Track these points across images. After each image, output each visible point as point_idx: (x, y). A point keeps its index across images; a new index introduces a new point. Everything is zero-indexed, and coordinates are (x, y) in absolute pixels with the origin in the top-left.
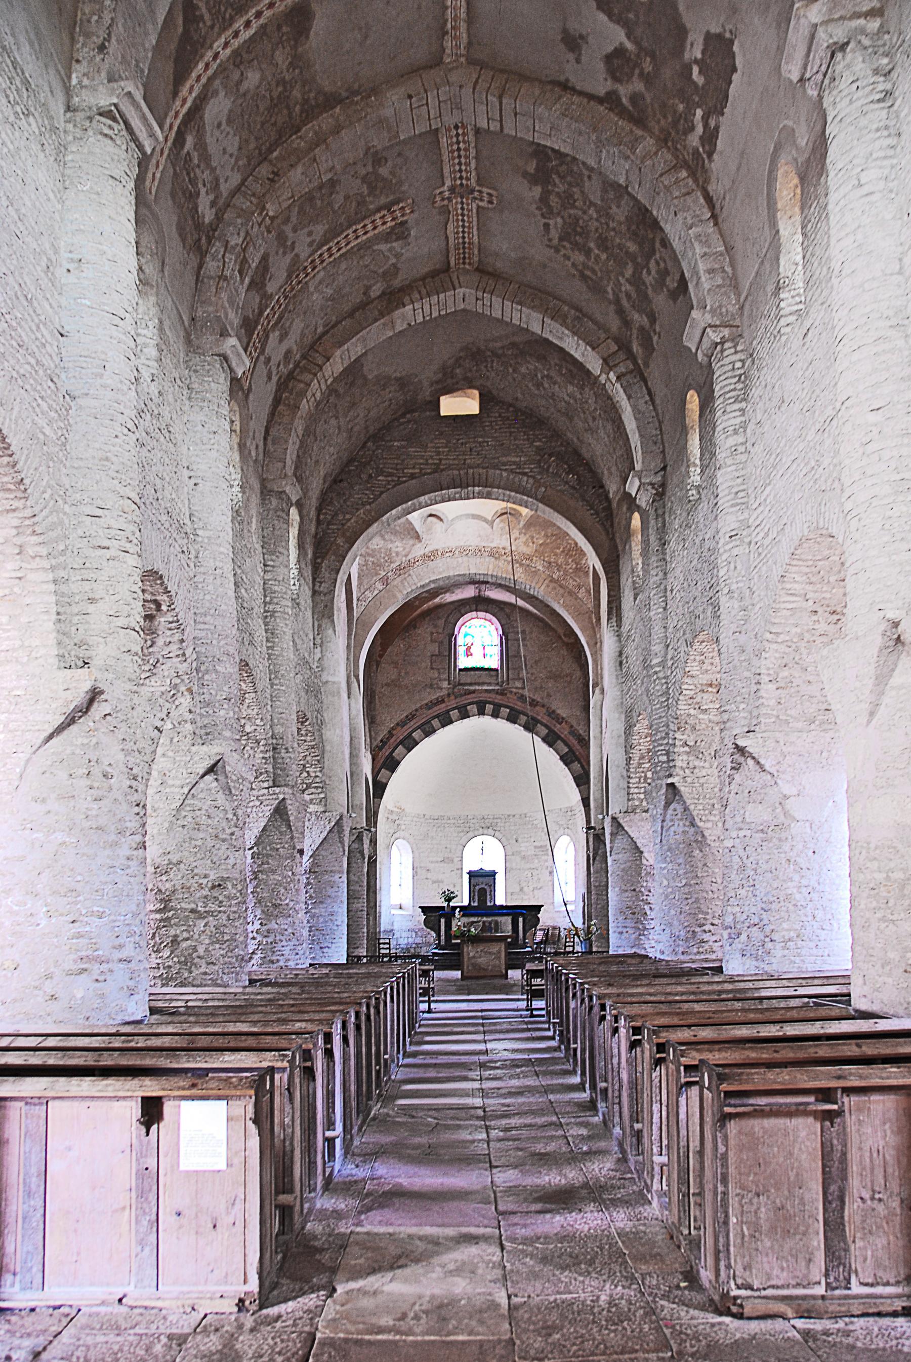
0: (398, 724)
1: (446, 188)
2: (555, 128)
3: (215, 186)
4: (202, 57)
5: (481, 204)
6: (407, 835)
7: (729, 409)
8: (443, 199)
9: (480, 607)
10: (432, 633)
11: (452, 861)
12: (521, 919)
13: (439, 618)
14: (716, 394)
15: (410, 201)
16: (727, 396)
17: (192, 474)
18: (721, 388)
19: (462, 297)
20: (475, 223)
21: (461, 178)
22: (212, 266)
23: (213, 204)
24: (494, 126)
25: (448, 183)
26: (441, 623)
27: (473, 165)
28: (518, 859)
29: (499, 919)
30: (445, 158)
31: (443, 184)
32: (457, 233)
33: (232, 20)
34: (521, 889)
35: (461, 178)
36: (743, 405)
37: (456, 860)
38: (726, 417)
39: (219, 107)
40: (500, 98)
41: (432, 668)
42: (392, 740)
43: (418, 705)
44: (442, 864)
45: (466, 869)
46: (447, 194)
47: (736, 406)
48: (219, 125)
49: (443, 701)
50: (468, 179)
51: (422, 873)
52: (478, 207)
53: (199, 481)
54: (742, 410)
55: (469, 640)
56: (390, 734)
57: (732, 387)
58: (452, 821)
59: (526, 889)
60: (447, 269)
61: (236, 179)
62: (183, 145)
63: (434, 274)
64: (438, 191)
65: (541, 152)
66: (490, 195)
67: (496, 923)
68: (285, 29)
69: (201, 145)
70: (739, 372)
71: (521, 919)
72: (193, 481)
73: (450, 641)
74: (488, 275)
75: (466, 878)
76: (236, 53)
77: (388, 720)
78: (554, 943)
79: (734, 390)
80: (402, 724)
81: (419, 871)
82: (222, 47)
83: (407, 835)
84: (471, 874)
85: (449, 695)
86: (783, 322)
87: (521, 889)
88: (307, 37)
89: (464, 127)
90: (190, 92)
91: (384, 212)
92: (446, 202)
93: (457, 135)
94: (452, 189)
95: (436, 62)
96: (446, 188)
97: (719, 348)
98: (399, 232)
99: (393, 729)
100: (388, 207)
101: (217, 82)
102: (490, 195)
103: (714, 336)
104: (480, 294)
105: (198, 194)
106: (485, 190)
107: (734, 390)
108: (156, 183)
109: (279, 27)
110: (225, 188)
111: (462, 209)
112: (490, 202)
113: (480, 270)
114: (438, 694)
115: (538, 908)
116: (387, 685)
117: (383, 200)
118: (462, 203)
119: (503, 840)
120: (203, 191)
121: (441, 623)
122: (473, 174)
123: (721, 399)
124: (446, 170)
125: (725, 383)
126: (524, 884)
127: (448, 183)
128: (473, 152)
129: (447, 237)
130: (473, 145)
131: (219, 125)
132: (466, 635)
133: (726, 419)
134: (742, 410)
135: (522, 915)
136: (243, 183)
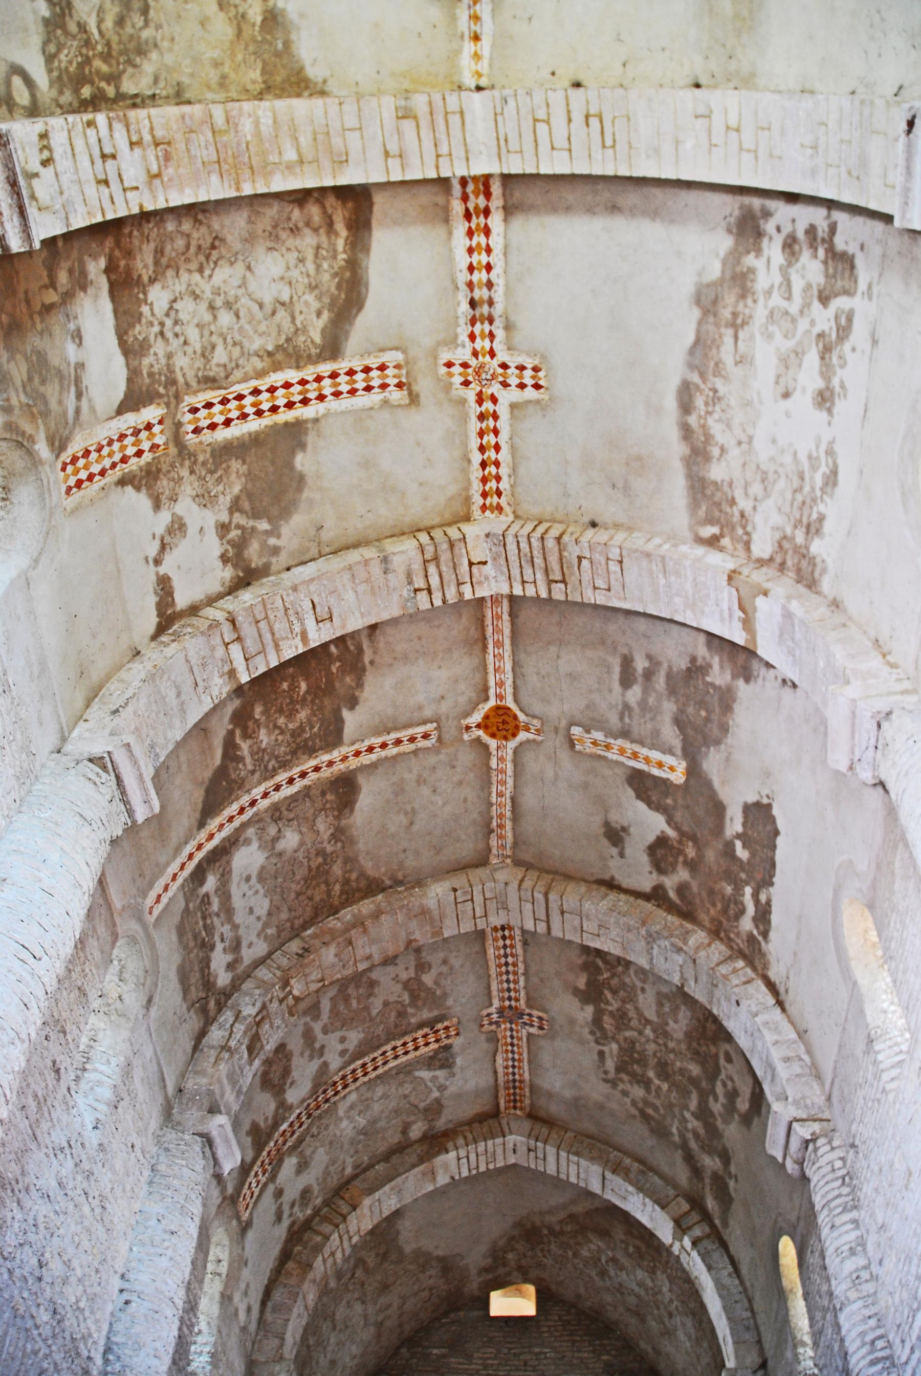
1: (493, 1010)
2: (606, 926)
3: (236, 946)
4: (237, 799)
5: (532, 1030)
7: (838, 1221)
8: (491, 1023)
14: (818, 1207)
15: (455, 1020)
16: (833, 1204)
17: (126, 1285)
18: (823, 1196)
19: (511, 1147)
20: (525, 1055)
21: (510, 999)
22: (216, 1035)
23: (230, 966)
24: (541, 928)
25: (496, 1003)
27: (522, 983)
30: (493, 971)
31: (491, 1005)
32: (506, 1067)
33: (274, 773)
35: (510, 999)
36: (854, 1214)
38: (835, 1234)
39: (248, 859)
40: (546, 895)
46: (495, 1017)
47: (847, 1217)
48: (248, 879)
50: (517, 1000)
52: (529, 1035)
53: (134, 1298)
54: (855, 1222)
57: (836, 1192)
60: (495, 1113)
61: (261, 948)
62: (202, 882)
63: (480, 1118)
64: (485, 1012)
65: (593, 960)
66: (540, 1018)
68: (329, 797)
69: (224, 892)
70: (844, 1172)
72: (125, 1296)
74: (541, 1121)
76: (275, 808)
79: (839, 1196)
82: (260, 795)
86: (886, 1077)
88: (352, 811)
89: (511, 928)
90: (219, 828)
91: (426, 1030)
92: (493, 1027)
93: (505, 947)
94: (501, 1011)
95: (482, 861)
96: (493, 1010)
97: (811, 1146)
98: (442, 1059)
100: (431, 1024)
101: (251, 832)
102: (540, 1018)
103: (803, 1131)
104: (532, 1142)
105: (212, 947)
106: (535, 1013)
107: (839, 1196)
108: (161, 906)
109: (323, 793)
110: (248, 955)
111: (512, 1037)
112: (541, 1028)
113: (533, 1116)
117: (426, 1015)
118: (511, 1030)
120: (219, 947)
122: (523, 993)
123: (825, 1212)
124: (494, 987)
125: (827, 1188)
127: (496, 1003)
128: (521, 968)
129: (495, 1072)
130: (521, 959)
131: (248, 879)
133: (835, 1236)
134: (855, 1222)
136: (269, 955)
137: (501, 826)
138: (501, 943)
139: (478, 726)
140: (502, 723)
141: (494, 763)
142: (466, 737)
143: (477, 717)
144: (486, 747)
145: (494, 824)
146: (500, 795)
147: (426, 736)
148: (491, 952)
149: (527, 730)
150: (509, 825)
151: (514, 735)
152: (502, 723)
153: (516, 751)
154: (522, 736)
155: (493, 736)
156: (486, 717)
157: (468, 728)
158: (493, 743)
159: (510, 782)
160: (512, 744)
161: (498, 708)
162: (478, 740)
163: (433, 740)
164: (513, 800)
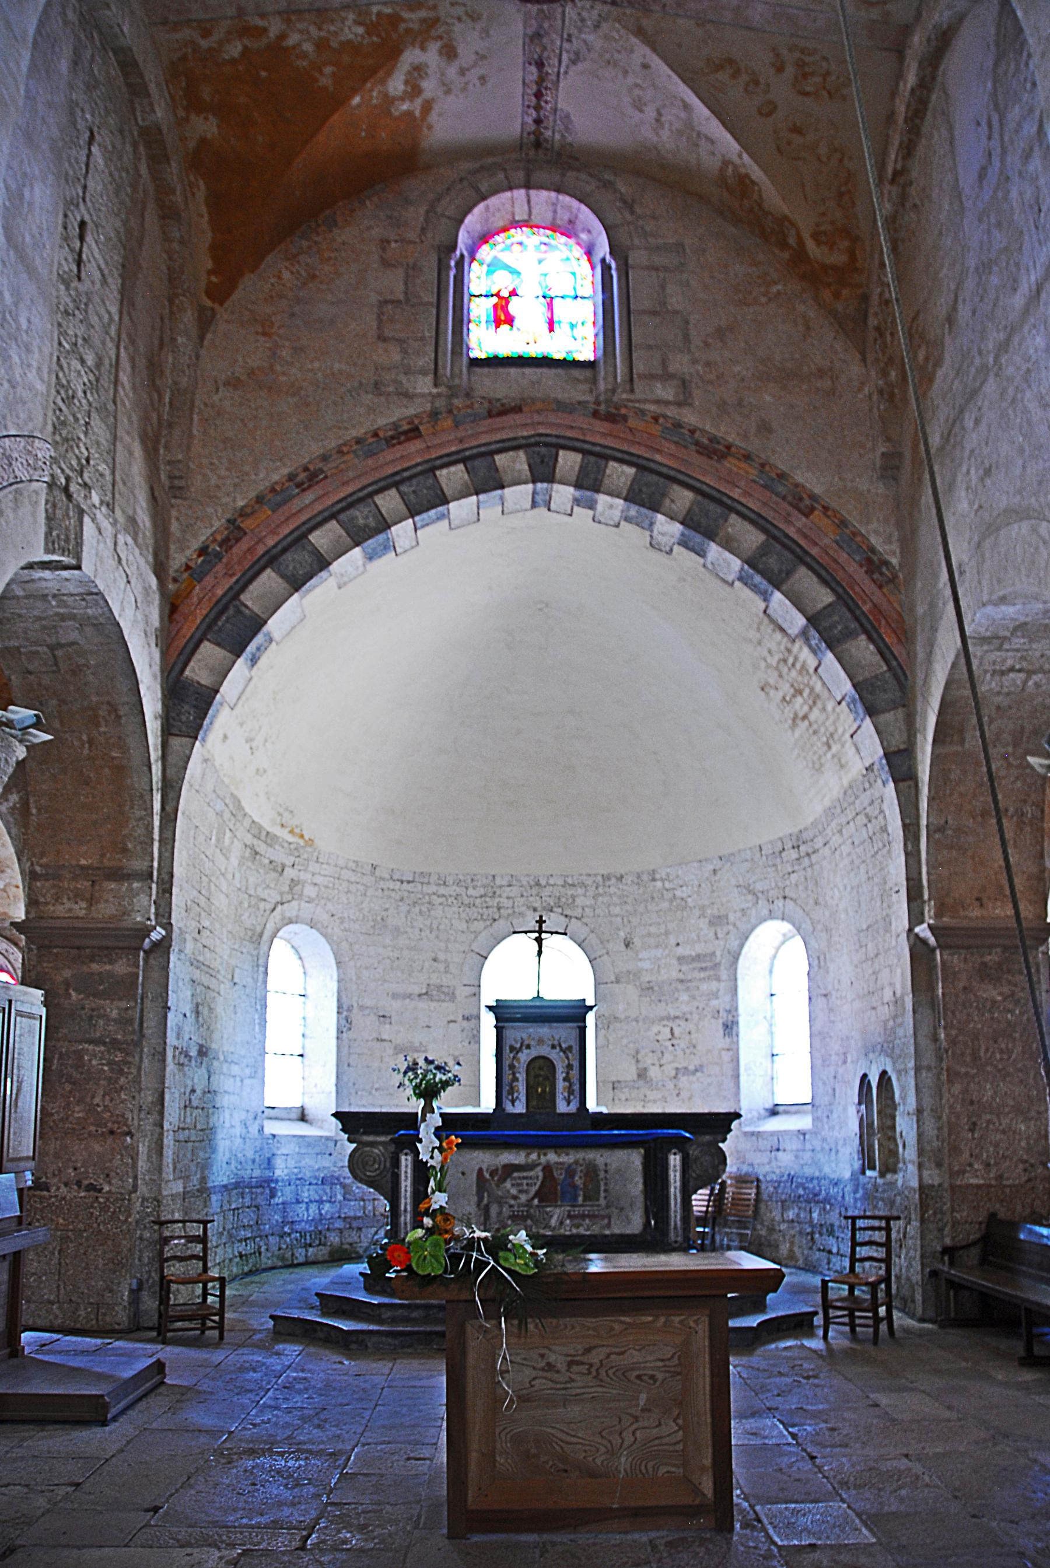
0: (260, 500)
6: (324, 917)
9: (538, 176)
10: (384, 242)
11: (452, 997)
12: (675, 1160)
13: (408, 202)
26: (415, 215)
28: (632, 992)
29: (599, 1157)
34: (642, 1074)
37: (462, 992)
41: (382, 338)
42: (238, 549)
43: (332, 444)
44: (423, 1004)
45: (488, 998)
49: (413, 433)
51: (366, 1025)
55: (502, 282)
56: (234, 532)
58: (453, 890)
59: (654, 1072)
67: (591, 1171)
71: (675, 1160)
73: (442, 268)
75: (488, 1021)
77: (227, 489)
78: (741, 1224)
80: (273, 498)
81: (356, 1015)
83: (324, 917)
84: (505, 1013)
85: (434, 415)
87: (642, 1074)
99: (243, 513)
114: (399, 412)
115: (720, 1124)
116: (234, 383)
119: (593, 939)
121: (415, 215)
126: (648, 1060)
132: (494, 266)
135: (681, 1144)
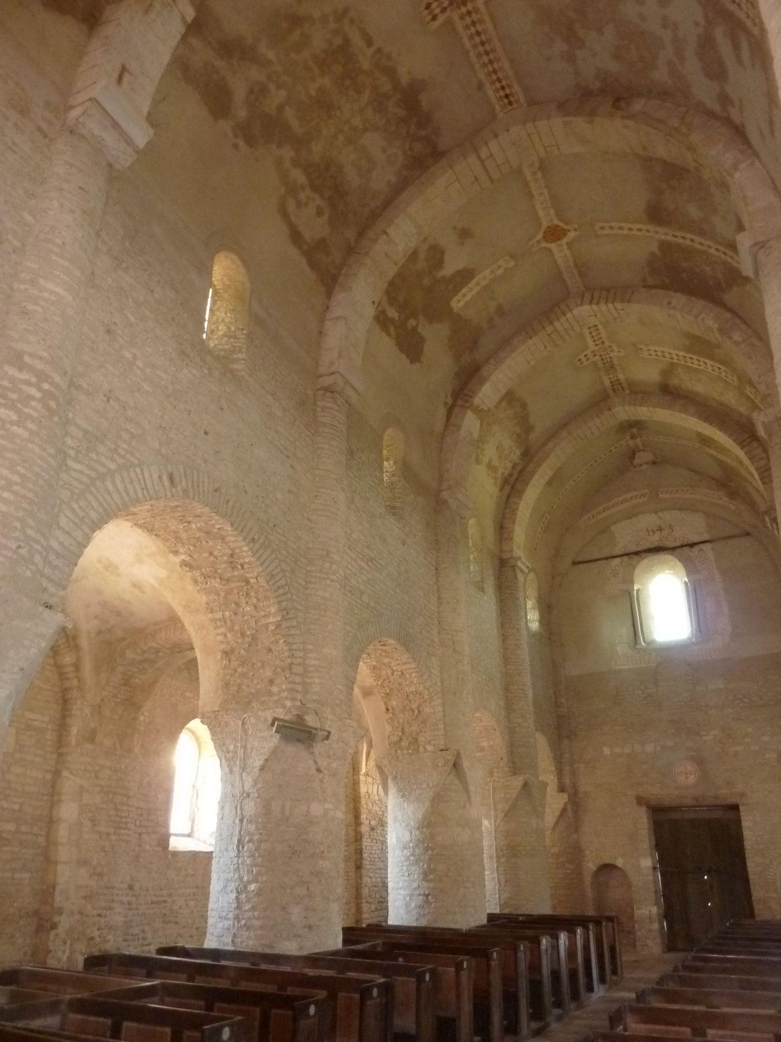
50: (462, 17)
124: (489, 26)
137: (534, 173)
138: (500, 75)
139: (569, 231)
140: (554, 234)
141: (552, 212)
142: (576, 226)
143: (572, 235)
144: (561, 220)
145: (539, 174)
146: (541, 194)
147: (602, 228)
148: (507, 66)
149: (539, 242)
150: (529, 177)
151: (545, 232)
152: (554, 234)
153: (540, 225)
154: (539, 236)
155: (557, 226)
156: (565, 235)
157: (576, 230)
158: (556, 222)
159: (538, 206)
160: (545, 224)
161: (559, 239)
162: (566, 224)
163: (598, 225)
164: (531, 195)
